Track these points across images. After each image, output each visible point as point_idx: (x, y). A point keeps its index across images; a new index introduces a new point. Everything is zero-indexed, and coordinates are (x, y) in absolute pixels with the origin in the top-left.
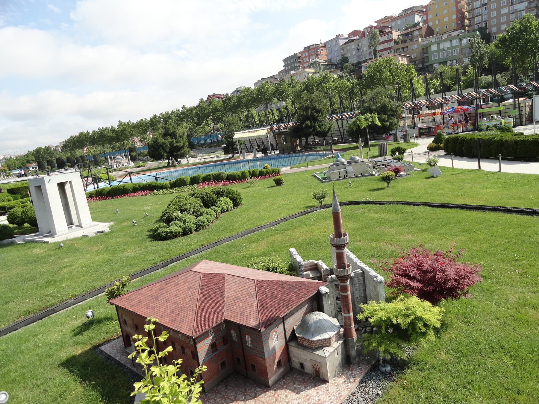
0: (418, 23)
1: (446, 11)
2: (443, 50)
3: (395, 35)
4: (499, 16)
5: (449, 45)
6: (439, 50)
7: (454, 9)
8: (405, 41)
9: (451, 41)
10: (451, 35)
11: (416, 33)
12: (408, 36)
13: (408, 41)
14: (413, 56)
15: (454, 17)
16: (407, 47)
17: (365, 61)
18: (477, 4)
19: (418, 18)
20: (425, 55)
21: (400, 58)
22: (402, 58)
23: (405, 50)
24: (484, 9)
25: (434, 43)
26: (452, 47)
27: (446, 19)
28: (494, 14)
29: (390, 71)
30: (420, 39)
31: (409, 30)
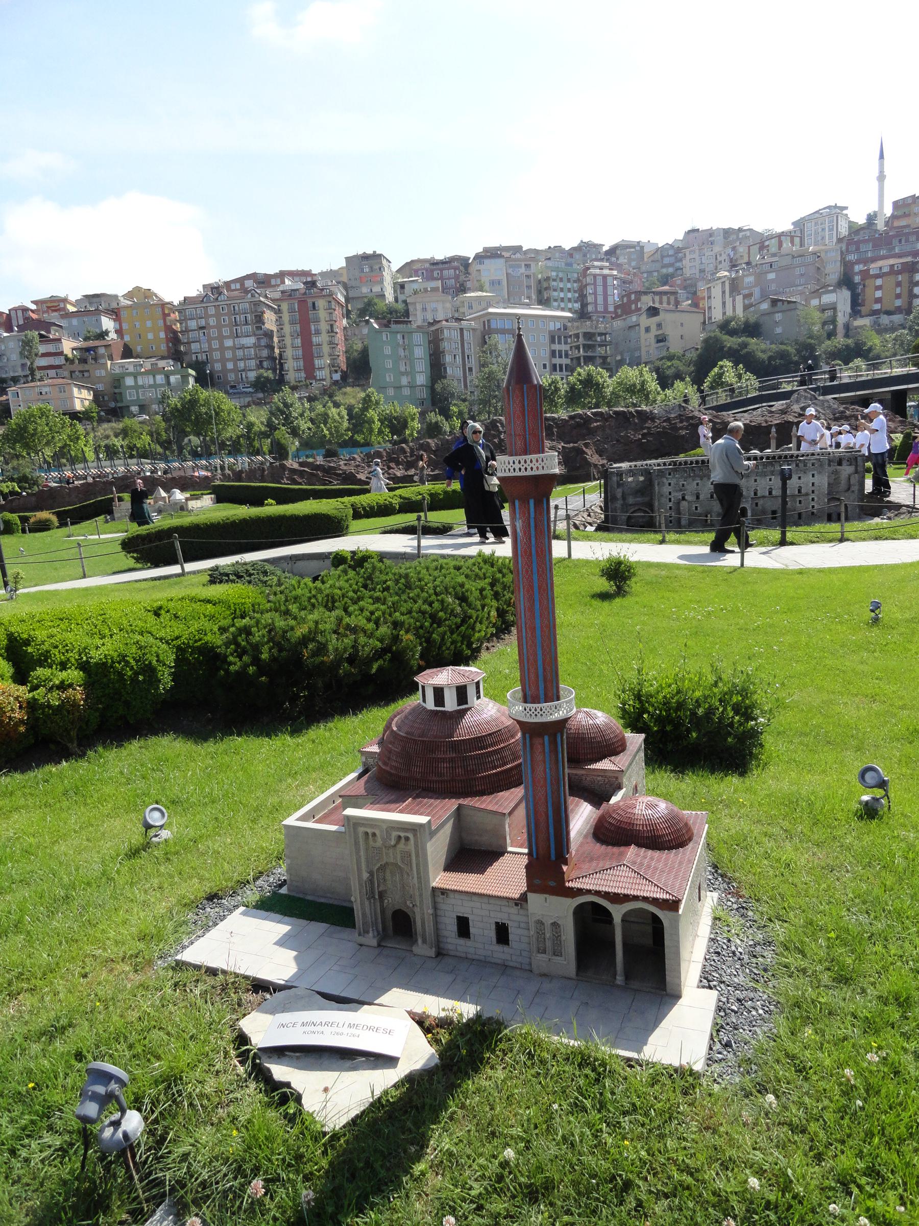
0: (107, 333)
1: (149, 324)
2: (143, 387)
3: (68, 346)
4: (222, 349)
5: (152, 382)
6: (136, 387)
7: (161, 323)
8: (83, 361)
9: (154, 376)
10: (156, 364)
11: (102, 351)
12: (88, 355)
13: (90, 361)
14: (100, 387)
15: (162, 335)
16: (88, 371)
17: (15, 380)
18: (193, 324)
19: (107, 323)
20: (117, 391)
21: (75, 390)
22: (79, 389)
23: (86, 374)
24: (202, 335)
25: (130, 374)
26: (155, 386)
27: (150, 336)
28: (215, 344)
29: (47, 425)
30: (109, 362)
31: (91, 343)
